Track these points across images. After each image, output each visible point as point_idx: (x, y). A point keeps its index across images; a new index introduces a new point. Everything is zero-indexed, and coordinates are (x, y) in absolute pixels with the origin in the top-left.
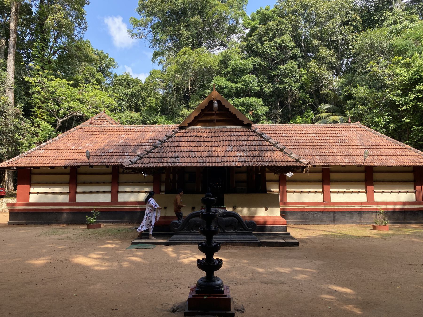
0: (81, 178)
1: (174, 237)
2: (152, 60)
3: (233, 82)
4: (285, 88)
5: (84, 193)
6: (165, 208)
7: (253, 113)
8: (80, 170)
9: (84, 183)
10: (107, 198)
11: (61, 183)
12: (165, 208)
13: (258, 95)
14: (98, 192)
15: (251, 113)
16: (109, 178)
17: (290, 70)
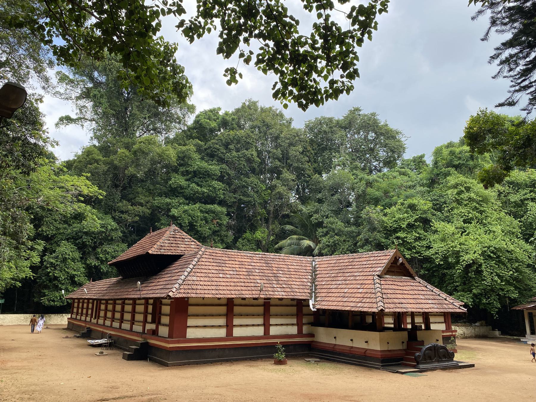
0: (236, 309)
1: (421, 366)
2: (57, 125)
3: (198, 185)
4: (249, 202)
5: (241, 326)
6: (388, 343)
7: (217, 222)
8: (236, 302)
9: (241, 315)
10: (260, 331)
11: (220, 315)
12: (388, 343)
13: (221, 203)
14: (253, 325)
15: (215, 222)
16: (261, 310)
17: (255, 185)
